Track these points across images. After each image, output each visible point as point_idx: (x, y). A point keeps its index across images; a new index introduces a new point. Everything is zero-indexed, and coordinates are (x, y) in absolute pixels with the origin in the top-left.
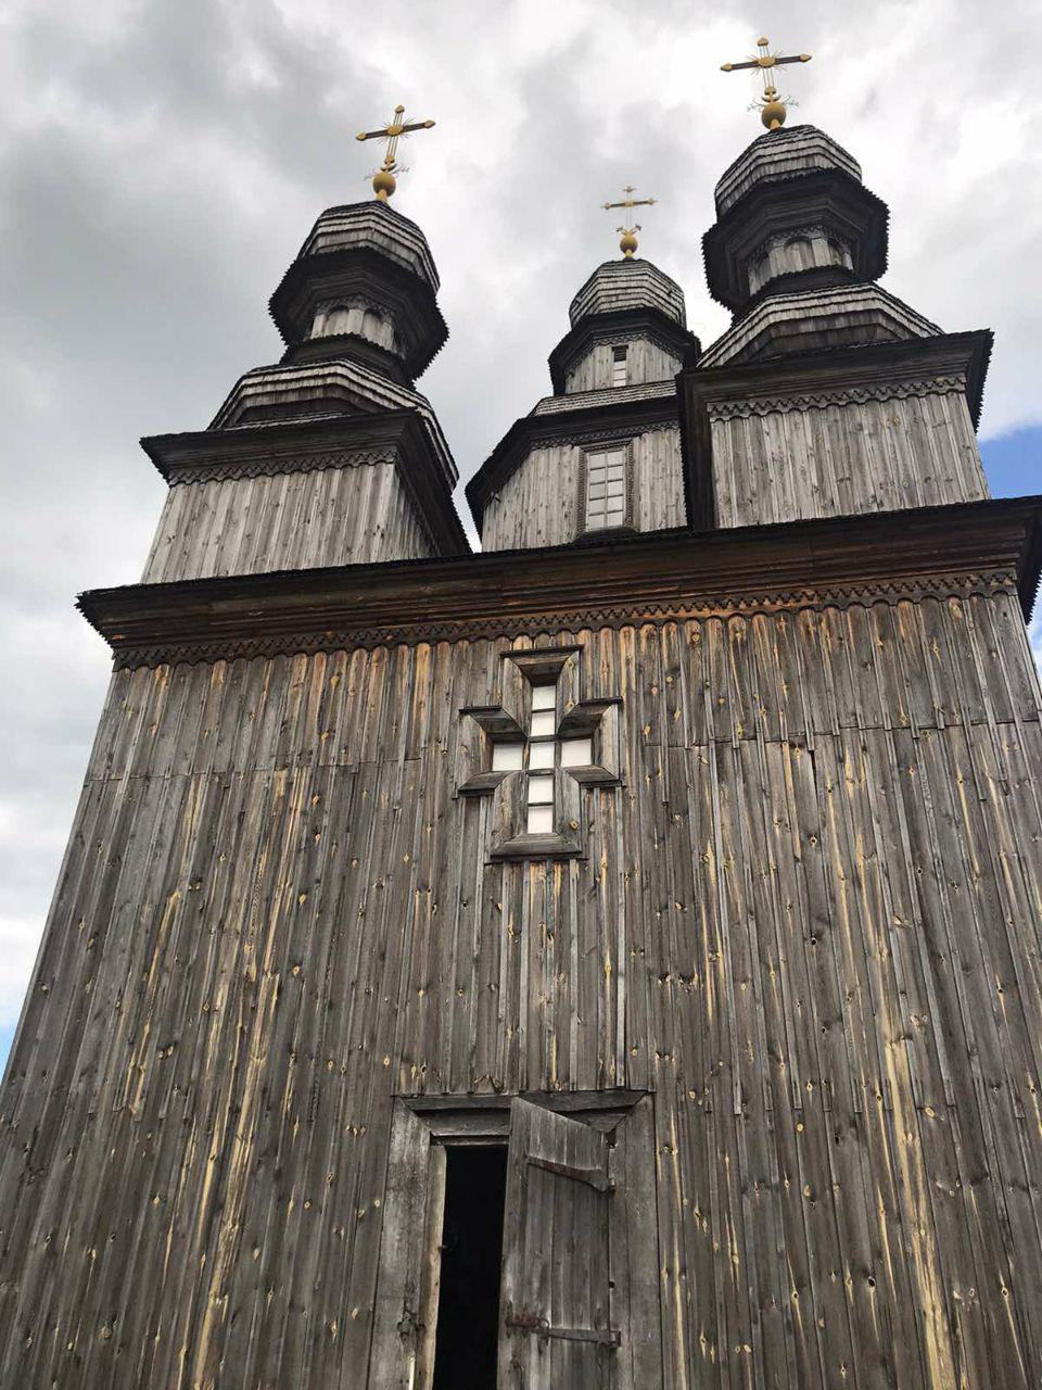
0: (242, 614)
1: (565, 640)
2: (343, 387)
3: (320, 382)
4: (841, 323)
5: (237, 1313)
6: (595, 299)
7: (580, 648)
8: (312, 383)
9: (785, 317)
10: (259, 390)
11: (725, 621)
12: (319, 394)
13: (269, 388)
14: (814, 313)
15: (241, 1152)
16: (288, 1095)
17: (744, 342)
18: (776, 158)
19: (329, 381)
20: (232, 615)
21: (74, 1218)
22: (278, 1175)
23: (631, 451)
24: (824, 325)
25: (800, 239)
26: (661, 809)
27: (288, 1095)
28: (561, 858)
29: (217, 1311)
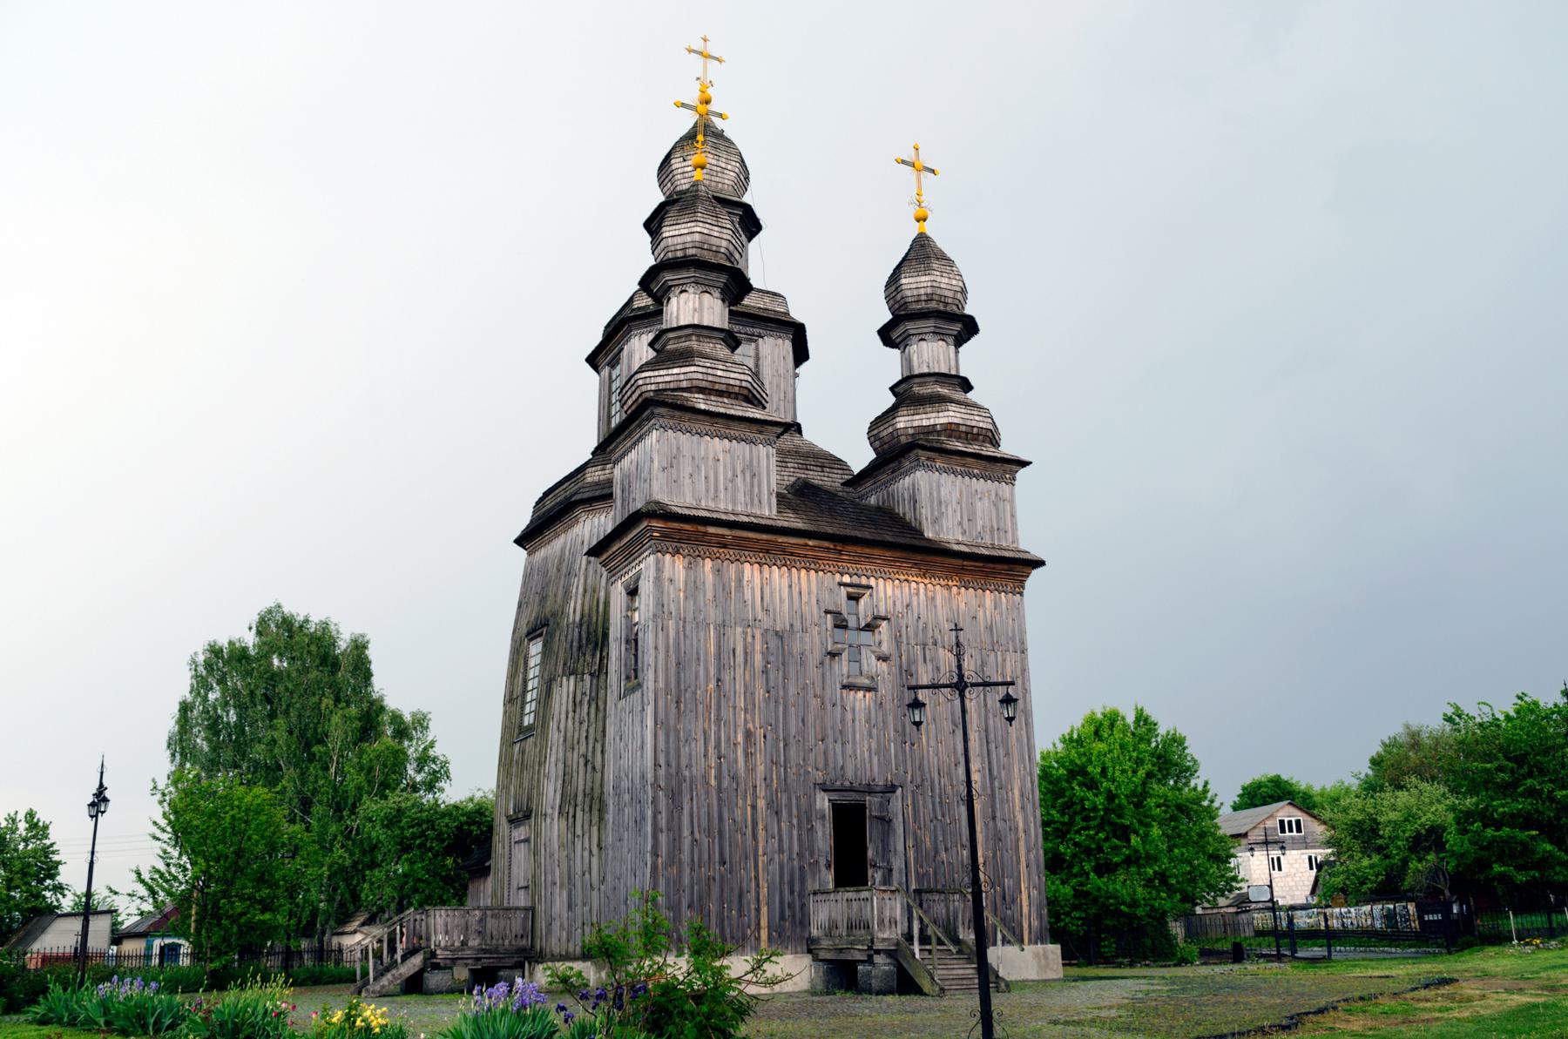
0: (723, 536)
1: (864, 581)
2: (749, 390)
3: (738, 383)
4: (975, 430)
5: (771, 860)
7: (871, 587)
8: (732, 382)
9: (956, 421)
10: (705, 377)
11: (925, 585)
12: (737, 390)
13: (710, 378)
14: (969, 423)
15: (761, 804)
16: (775, 781)
18: (942, 286)
19: (744, 384)
20: (716, 535)
21: (699, 826)
22: (777, 813)
23: (757, 348)
24: (969, 430)
25: (943, 340)
26: (904, 673)
27: (775, 781)
28: (869, 689)
29: (763, 862)
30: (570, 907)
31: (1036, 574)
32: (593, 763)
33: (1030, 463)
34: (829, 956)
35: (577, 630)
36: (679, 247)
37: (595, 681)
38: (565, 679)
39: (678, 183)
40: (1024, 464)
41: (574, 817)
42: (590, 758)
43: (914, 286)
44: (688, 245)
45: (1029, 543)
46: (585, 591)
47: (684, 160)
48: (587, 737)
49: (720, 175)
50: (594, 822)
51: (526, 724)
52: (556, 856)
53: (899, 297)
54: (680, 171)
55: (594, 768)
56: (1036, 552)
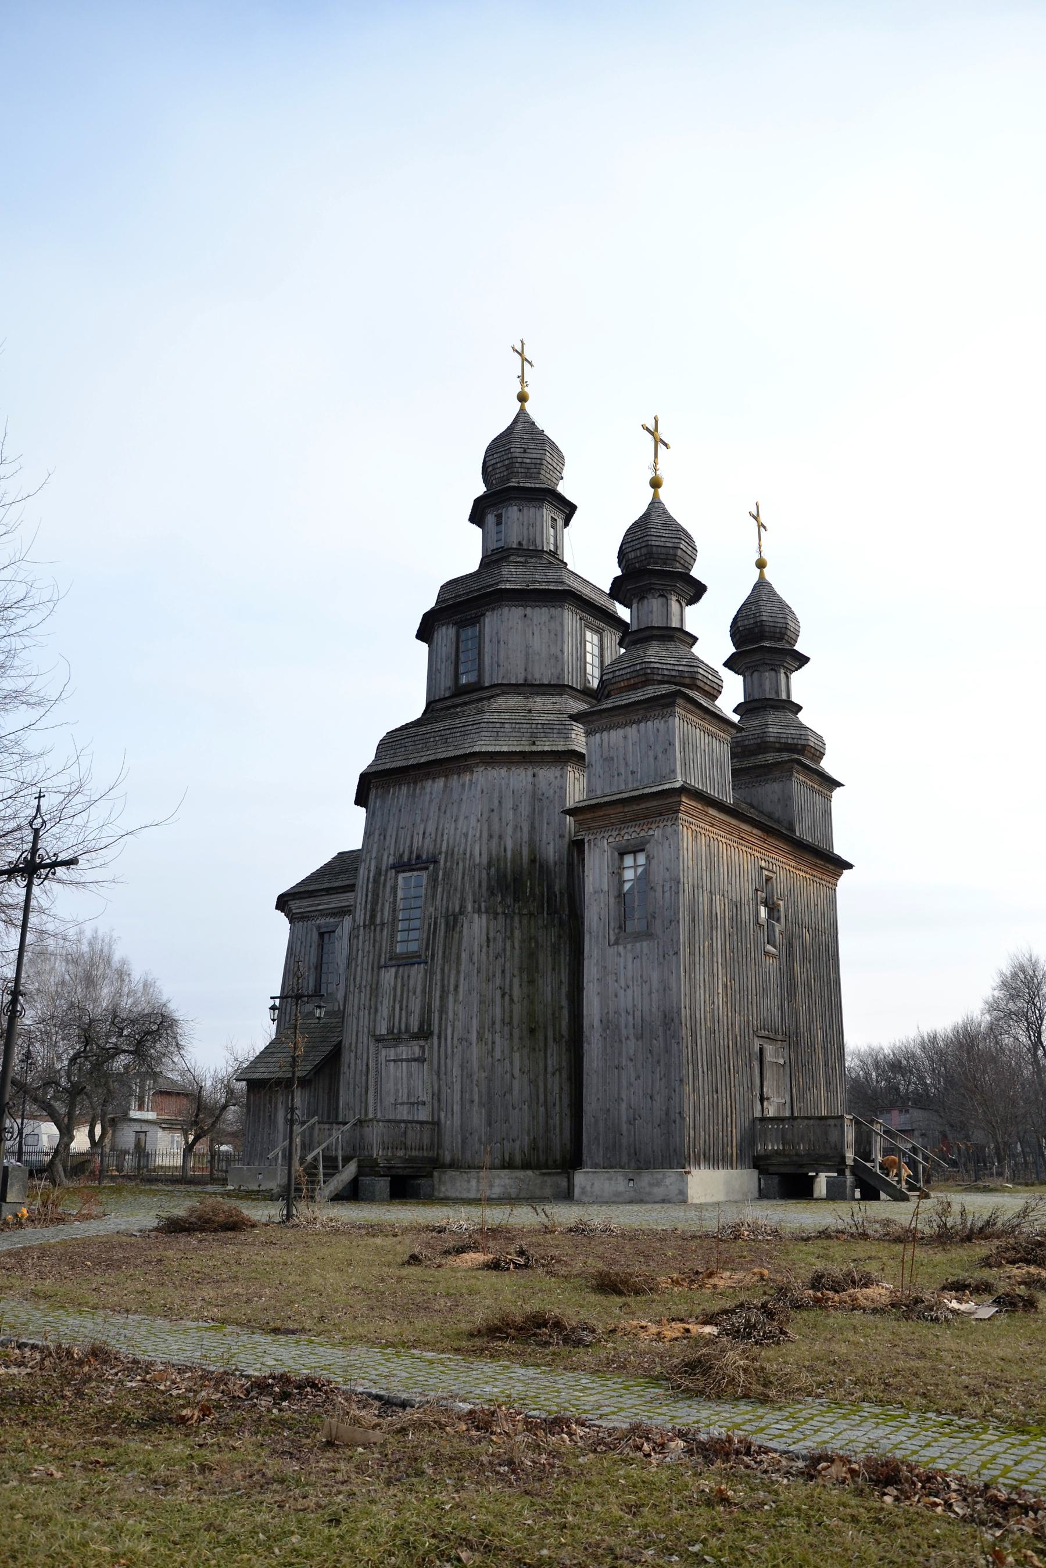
6: (538, 461)
17: (795, 741)
30: (489, 1124)
31: (846, 873)
32: (511, 996)
33: (843, 785)
34: (784, 1170)
35: (485, 872)
36: (662, 557)
37: (508, 921)
38: (476, 916)
39: (515, 470)
40: (840, 785)
41: (493, 1043)
42: (507, 990)
43: (772, 624)
44: (669, 557)
45: (840, 849)
46: (491, 836)
47: (525, 452)
48: (503, 972)
49: (551, 473)
50: (515, 1048)
51: (398, 951)
52: (475, 1078)
53: (756, 630)
54: (519, 460)
55: (512, 1000)
56: (845, 857)
